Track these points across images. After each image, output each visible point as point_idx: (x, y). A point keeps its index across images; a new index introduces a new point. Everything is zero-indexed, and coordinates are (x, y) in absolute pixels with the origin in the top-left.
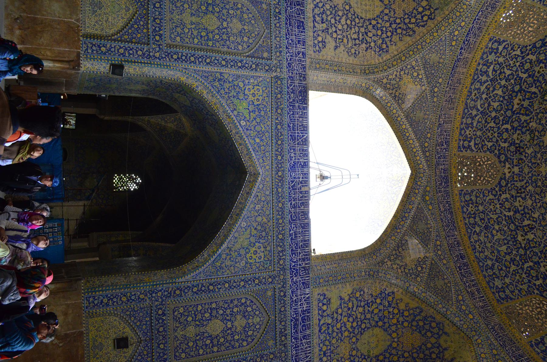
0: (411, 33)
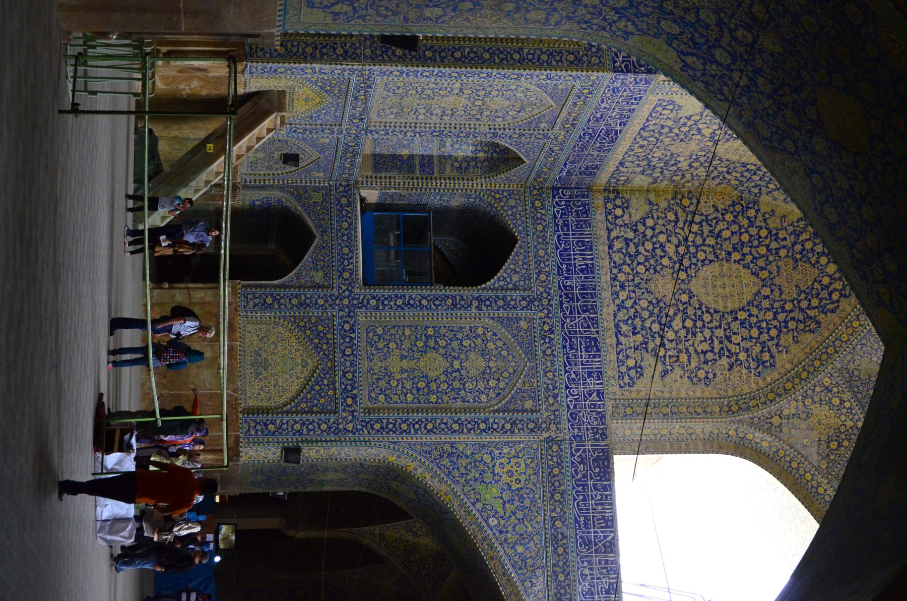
0: (813, 326)
